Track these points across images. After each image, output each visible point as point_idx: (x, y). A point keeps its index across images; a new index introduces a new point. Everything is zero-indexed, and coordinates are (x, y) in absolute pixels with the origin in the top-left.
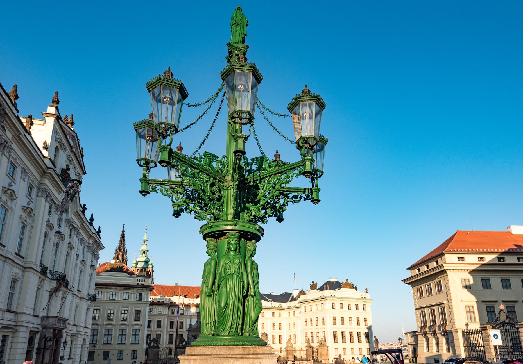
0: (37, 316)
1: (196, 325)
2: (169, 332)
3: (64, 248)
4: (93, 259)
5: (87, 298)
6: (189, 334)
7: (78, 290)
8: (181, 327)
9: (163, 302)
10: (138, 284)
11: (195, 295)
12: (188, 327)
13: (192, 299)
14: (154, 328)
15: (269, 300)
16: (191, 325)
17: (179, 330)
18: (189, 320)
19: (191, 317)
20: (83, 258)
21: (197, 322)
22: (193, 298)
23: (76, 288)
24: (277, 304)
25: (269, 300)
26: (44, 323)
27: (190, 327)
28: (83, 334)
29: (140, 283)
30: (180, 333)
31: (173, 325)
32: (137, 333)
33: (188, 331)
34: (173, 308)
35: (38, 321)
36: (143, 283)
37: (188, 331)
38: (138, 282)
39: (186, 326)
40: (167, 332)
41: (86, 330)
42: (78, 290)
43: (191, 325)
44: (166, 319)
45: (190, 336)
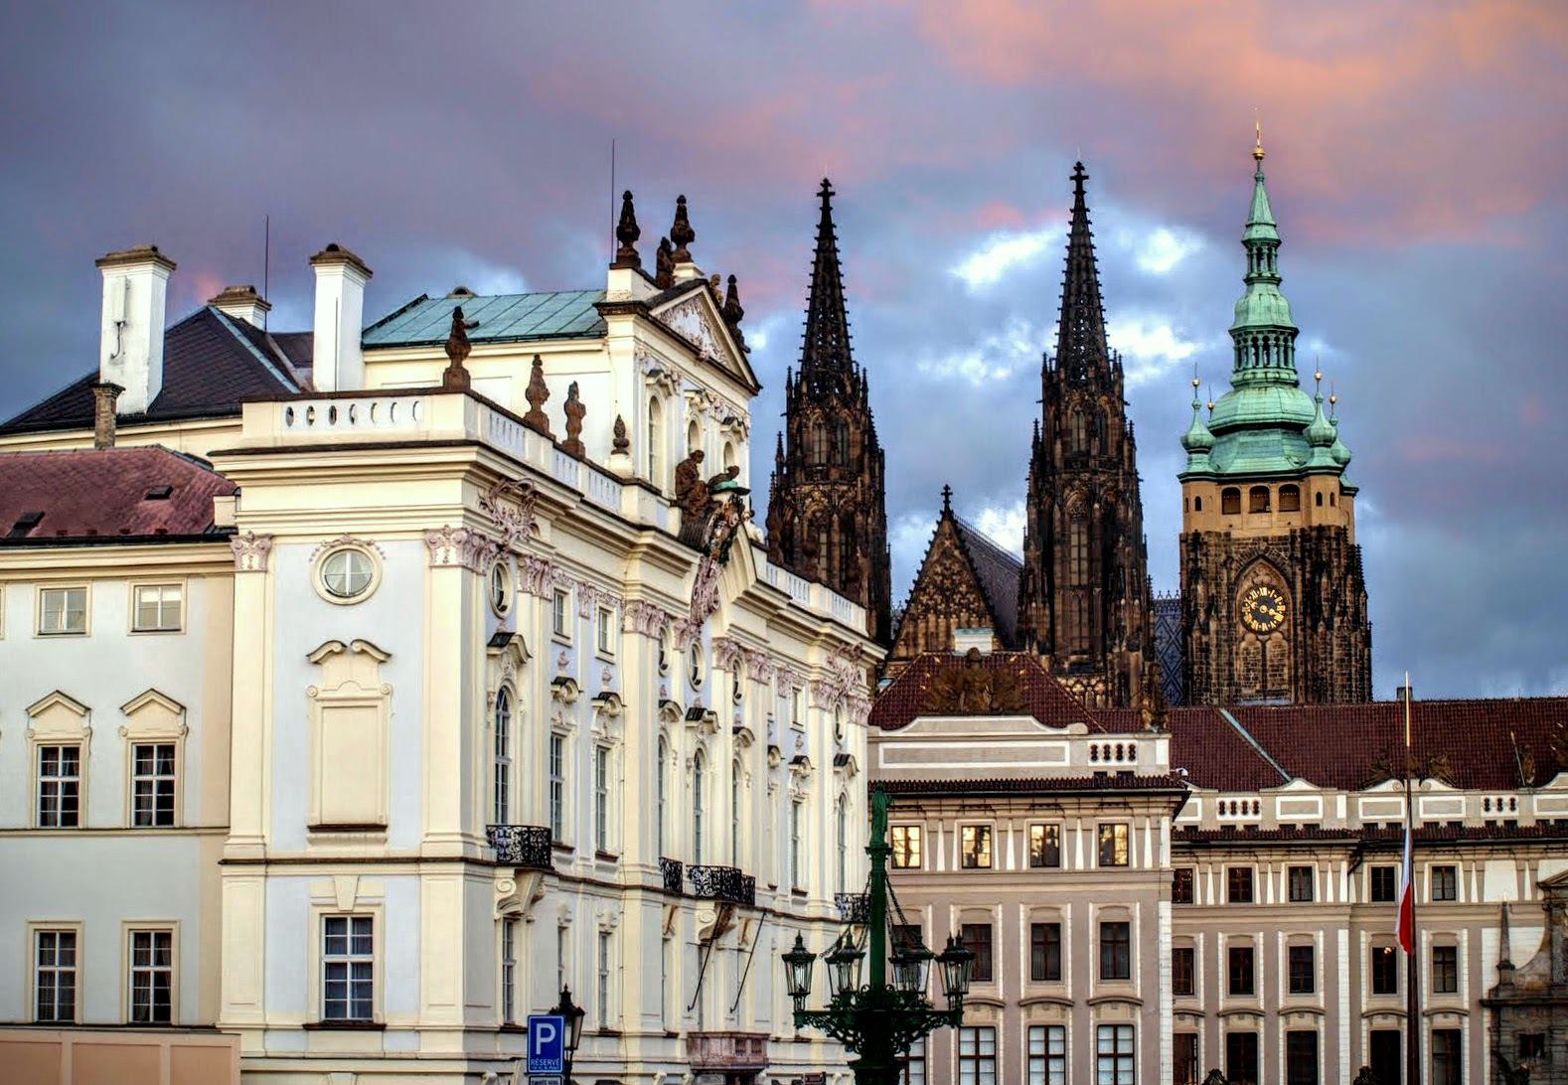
0: (671, 1036)
1: (1543, 967)
2: (1369, 1016)
3: (721, 749)
4: (843, 721)
5: (834, 913)
6: (1496, 1029)
7: (795, 892)
8: (1447, 980)
9: (1311, 828)
10: (1100, 775)
11: (1528, 767)
12: (1489, 980)
13: (1506, 798)
14: (1271, 998)
16: (1504, 966)
18: (1490, 937)
19: (1504, 917)
20: (799, 746)
21: (1548, 943)
22: (1511, 783)
23: (784, 888)
26: (698, 1057)
27: (1503, 984)
29: (1112, 767)
30: (1440, 1022)
32: (1124, 1048)
33: (1493, 1004)
34: (1382, 861)
35: (678, 1050)
36: (1126, 764)
38: (1101, 764)
39: (1479, 975)
40: (1356, 1016)
42: (795, 892)
44: (1343, 936)
45: (1507, 1039)
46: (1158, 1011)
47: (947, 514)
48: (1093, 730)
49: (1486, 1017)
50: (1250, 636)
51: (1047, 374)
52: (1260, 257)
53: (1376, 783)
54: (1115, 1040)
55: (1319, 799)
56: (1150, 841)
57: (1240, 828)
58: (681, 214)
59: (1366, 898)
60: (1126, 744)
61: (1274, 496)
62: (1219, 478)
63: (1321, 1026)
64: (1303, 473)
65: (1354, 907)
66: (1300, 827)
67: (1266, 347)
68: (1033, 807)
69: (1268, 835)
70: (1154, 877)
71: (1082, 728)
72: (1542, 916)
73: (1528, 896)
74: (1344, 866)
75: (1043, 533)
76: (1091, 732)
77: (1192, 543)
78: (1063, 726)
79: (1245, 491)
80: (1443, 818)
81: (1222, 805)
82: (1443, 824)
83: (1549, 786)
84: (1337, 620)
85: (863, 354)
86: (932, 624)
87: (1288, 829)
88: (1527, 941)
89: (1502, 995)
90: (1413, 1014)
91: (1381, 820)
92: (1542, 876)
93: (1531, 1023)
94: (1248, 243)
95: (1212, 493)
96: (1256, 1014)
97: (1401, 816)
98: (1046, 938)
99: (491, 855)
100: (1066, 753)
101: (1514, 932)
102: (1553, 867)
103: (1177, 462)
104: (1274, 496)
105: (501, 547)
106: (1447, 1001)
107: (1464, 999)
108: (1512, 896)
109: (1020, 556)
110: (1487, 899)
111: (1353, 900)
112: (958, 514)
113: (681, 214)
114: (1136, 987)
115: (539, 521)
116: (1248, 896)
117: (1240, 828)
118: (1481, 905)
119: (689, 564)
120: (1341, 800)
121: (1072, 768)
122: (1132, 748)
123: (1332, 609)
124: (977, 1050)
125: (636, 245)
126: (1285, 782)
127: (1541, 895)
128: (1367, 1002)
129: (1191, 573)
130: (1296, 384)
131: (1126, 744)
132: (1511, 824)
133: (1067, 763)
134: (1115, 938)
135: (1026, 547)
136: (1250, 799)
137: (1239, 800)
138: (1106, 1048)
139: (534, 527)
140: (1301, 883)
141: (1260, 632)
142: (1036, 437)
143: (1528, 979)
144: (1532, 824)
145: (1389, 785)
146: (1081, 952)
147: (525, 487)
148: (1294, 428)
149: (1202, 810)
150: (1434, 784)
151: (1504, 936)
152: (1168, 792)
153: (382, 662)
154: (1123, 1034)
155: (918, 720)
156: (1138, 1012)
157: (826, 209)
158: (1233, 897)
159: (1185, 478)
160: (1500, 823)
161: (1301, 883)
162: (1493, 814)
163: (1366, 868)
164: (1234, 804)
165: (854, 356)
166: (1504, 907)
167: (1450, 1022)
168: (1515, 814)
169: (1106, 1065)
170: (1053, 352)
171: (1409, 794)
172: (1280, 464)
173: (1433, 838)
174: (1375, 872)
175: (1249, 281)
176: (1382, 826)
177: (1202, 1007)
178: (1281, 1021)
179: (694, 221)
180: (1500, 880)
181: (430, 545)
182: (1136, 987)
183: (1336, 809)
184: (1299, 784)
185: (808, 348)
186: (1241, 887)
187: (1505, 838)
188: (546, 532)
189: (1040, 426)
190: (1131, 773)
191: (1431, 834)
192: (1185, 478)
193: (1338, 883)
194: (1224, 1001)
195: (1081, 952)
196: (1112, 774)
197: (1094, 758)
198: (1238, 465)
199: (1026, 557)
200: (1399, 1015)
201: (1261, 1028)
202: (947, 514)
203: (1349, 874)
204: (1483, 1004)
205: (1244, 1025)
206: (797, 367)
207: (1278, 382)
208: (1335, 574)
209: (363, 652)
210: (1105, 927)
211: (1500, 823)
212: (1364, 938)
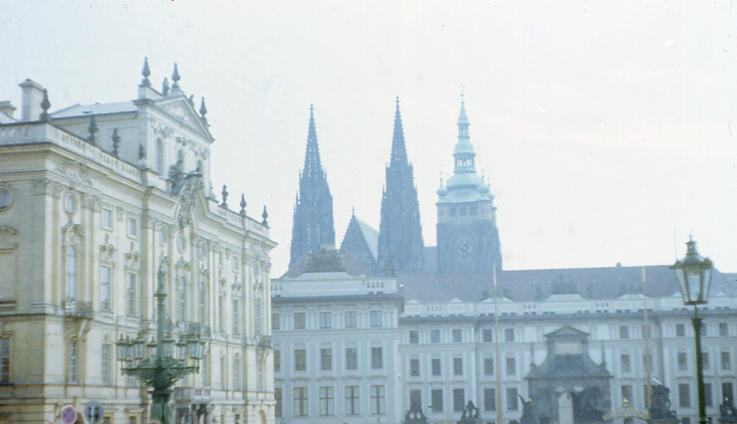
6: (530, 388)
12: (527, 370)
13: (532, 304)
16: (533, 365)
17: (504, 377)
18: (527, 354)
19: (532, 347)
21: (548, 355)
29: (375, 290)
33: (529, 379)
34: (487, 327)
36: (380, 289)
37: (529, 379)
38: (371, 290)
39: (523, 369)
41: (261, 396)
43: (533, 365)
44: (473, 354)
47: (353, 216)
49: (527, 383)
50: (460, 258)
52: (463, 129)
55: (464, 305)
56: (391, 318)
58: (176, 70)
59: (481, 340)
62: (449, 204)
63: (466, 388)
64: (476, 203)
65: (477, 344)
68: (346, 305)
71: (363, 276)
72: (546, 347)
73: (541, 340)
74: (473, 329)
77: (440, 227)
80: (509, 311)
81: (428, 307)
82: (509, 314)
85: (325, 164)
87: (452, 316)
89: (533, 376)
90: (498, 383)
91: (487, 312)
92: (546, 333)
93: (543, 385)
94: (459, 125)
95: (446, 209)
96: (442, 383)
97: (493, 311)
98: (351, 356)
101: (536, 353)
102: (550, 329)
103: (436, 199)
105: (71, 189)
106: (512, 378)
107: (518, 376)
108: (535, 339)
109: (378, 229)
111: (477, 341)
112: (356, 217)
113: (176, 70)
114: (384, 372)
115: (92, 180)
118: (523, 343)
119: (174, 203)
120: (471, 306)
122: (382, 284)
124: (327, 394)
125: (149, 77)
126: (450, 299)
127: (546, 339)
128: (483, 378)
129: (440, 237)
131: (380, 282)
132: (534, 313)
134: (377, 353)
136: (438, 306)
137: (435, 306)
139: (89, 182)
140: (457, 335)
141: (463, 256)
144: (541, 313)
145: (489, 300)
146: (364, 359)
147: (81, 164)
148: (474, 187)
149: (414, 308)
150: (505, 299)
151: (533, 354)
152: (398, 300)
153: (14, 234)
157: (312, 114)
159: (438, 205)
160: (530, 314)
161: (457, 335)
162: (527, 310)
163: (481, 331)
164: (432, 308)
165: (322, 164)
166: (532, 344)
167: (512, 386)
168: (535, 311)
170: (389, 161)
173: (507, 319)
174: (484, 331)
176: (487, 315)
179: (180, 73)
180: (531, 334)
181: (35, 186)
182: (384, 372)
183: (469, 309)
185: (307, 162)
186: (435, 338)
188: (96, 184)
189: (385, 186)
192: (438, 205)
193: (469, 335)
195: (364, 359)
196: (375, 293)
198: (454, 201)
199: (381, 231)
200: (493, 382)
202: (353, 216)
203: (475, 331)
204: (525, 378)
205: (437, 387)
206: (303, 168)
209: (6, 230)
210: (374, 349)
212: (481, 355)
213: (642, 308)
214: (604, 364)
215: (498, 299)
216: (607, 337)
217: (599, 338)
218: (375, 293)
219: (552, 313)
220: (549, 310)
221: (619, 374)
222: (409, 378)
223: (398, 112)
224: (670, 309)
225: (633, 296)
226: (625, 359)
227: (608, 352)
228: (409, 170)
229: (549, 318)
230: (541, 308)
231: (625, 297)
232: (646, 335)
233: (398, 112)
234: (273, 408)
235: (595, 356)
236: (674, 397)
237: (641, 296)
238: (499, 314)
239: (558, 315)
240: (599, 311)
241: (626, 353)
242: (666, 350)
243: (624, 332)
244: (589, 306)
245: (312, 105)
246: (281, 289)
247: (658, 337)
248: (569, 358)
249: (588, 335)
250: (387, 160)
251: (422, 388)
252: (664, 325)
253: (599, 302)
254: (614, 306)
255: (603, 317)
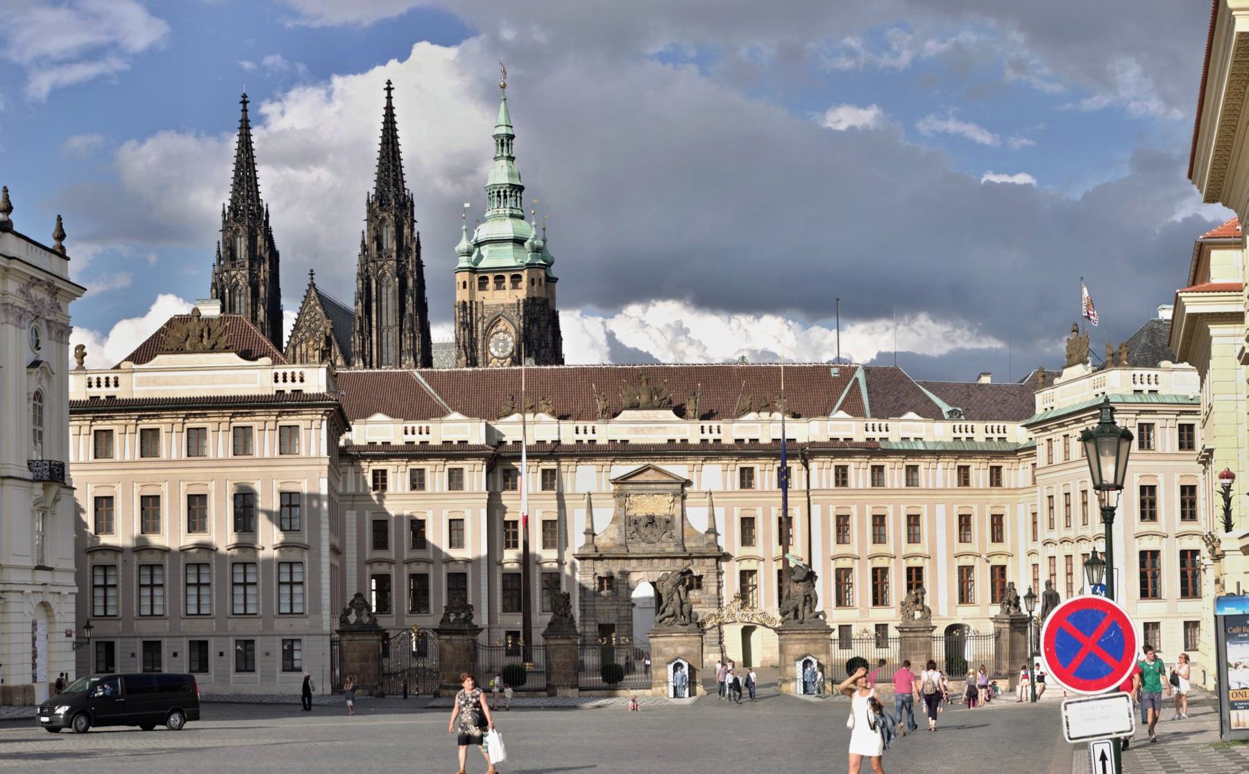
10: (280, 392)
13: (589, 425)
15: (946, 408)
16: (590, 533)
24: (980, 432)
25: (946, 408)
28: (28, 590)
29: (288, 387)
31: (515, 535)
36: (297, 385)
38: (281, 386)
46: (319, 554)
47: (312, 285)
48: (274, 363)
51: (369, 204)
53: (506, 416)
54: (291, 573)
57: (417, 443)
60: (297, 371)
61: (508, 279)
66: (455, 443)
67: (505, 197)
69: (434, 448)
70: (317, 462)
75: (366, 297)
76: (274, 363)
78: (255, 359)
79: (491, 277)
83: (617, 419)
84: (543, 351)
86: (304, 350)
88: (604, 517)
92: (614, 476)
99: (29, 475)
100: (256, 379)
104: (508, 279)
110: (577, 491)
116: (422, 487)
117: (417, 443)
121: (262, 388)
123: (540, 344)
127: (612, 487)
130: (522, 218)
132: (592, 442)
133: (258, 385)
135: (356, 304)
136: (424, 425)
138: (285, 578)
142: (363, 242)
143: (603, 541)
145: (516, 417)
154: (296, 569)
155: (159, 357)
156: (306, 554)
158: (413, 487)
160: (585, 442)
169: (285, 590)
170: (373, 192)
171: (524, 422)
172: (511, 262)
175: (496, 158)
177: (393, 557)
178: (444, 567)
180: (584, 478)
184: (456, 416)
187: (587, 452)
190: (300, 391)
191: (541, 448)
194: (407, 554)
196: (288, 392)
197: (276, 381)
201: (431, 571)
202: (312, 285)
205: (420, 569)
207: (512, 216)
208: (543, 324)
211: (585, 442)
213: (780, 436)
214: (713, 531)
215: (529, 417)
216: (717, 486)
217: (705, 488)
218: (288, 392)
219: (625, 442)
220: (619, 438)
221: (737, 550)
222: (369, 554)
223: (389, 109)
224: (825, 439)
225: (765, 415)
226: (748, 524)
227: (720, 512)
228: (405, 206)
229: (621, 451)
230: (605, 432)
231: (752, 416)
232: (784, 483)
233: (389, 109)
234: (73, 599)
235: (698, 519)
236: (824, 589)
237: (777, 416)
238: (531, 441)
239: (637, 446)
240: (704, 441)
241: (748, 514)
242: (816, 509)
243: (747, 478)
244: (691, 431)
245: (245, 96)
246: (116, 385)
247: (805, 488)
248: (652, 521)
249: (689, 483)
250: (369, 185)
251: (393, 571)
252: (813, 465)
253: (706, 424)
254: (730, 431)
255: (711, 451)
